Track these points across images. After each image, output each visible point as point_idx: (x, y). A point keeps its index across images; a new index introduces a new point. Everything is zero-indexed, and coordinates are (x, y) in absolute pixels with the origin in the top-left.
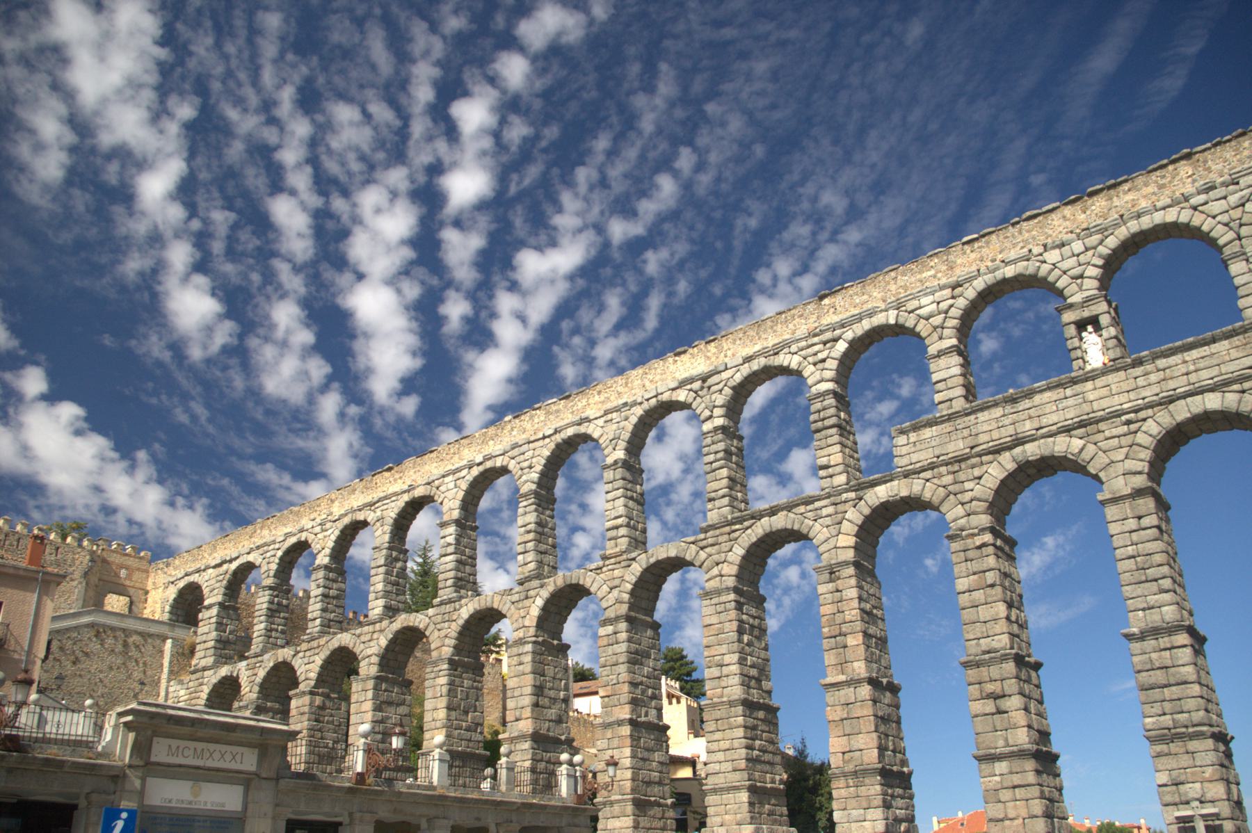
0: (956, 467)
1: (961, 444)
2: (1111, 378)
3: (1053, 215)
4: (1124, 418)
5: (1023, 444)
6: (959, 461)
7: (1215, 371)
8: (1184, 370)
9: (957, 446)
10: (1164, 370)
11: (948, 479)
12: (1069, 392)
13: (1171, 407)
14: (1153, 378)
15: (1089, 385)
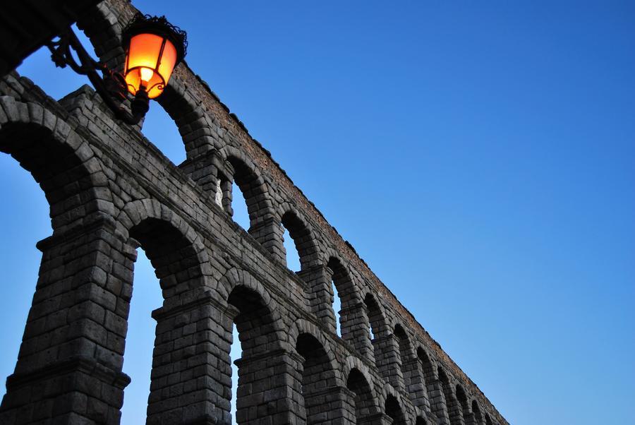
0: (121, 171)
1: (130, 160)
2: (222, 222)
3: (213, 101)
4: (226, 254)
5: (171, 207)
6: (125, 170)
7: (263, 273)
8: (252, 257)
9: (126, 156)
10: (244, 247)
11: (112, 175)
12: (201, 204)
13: (244, 271)
14: (240, 246)
15: (211, 214)
